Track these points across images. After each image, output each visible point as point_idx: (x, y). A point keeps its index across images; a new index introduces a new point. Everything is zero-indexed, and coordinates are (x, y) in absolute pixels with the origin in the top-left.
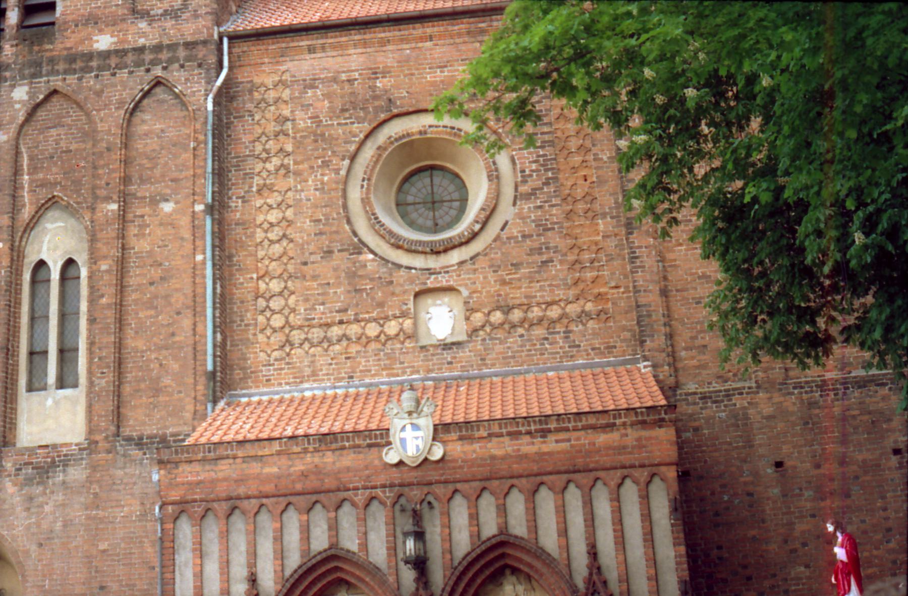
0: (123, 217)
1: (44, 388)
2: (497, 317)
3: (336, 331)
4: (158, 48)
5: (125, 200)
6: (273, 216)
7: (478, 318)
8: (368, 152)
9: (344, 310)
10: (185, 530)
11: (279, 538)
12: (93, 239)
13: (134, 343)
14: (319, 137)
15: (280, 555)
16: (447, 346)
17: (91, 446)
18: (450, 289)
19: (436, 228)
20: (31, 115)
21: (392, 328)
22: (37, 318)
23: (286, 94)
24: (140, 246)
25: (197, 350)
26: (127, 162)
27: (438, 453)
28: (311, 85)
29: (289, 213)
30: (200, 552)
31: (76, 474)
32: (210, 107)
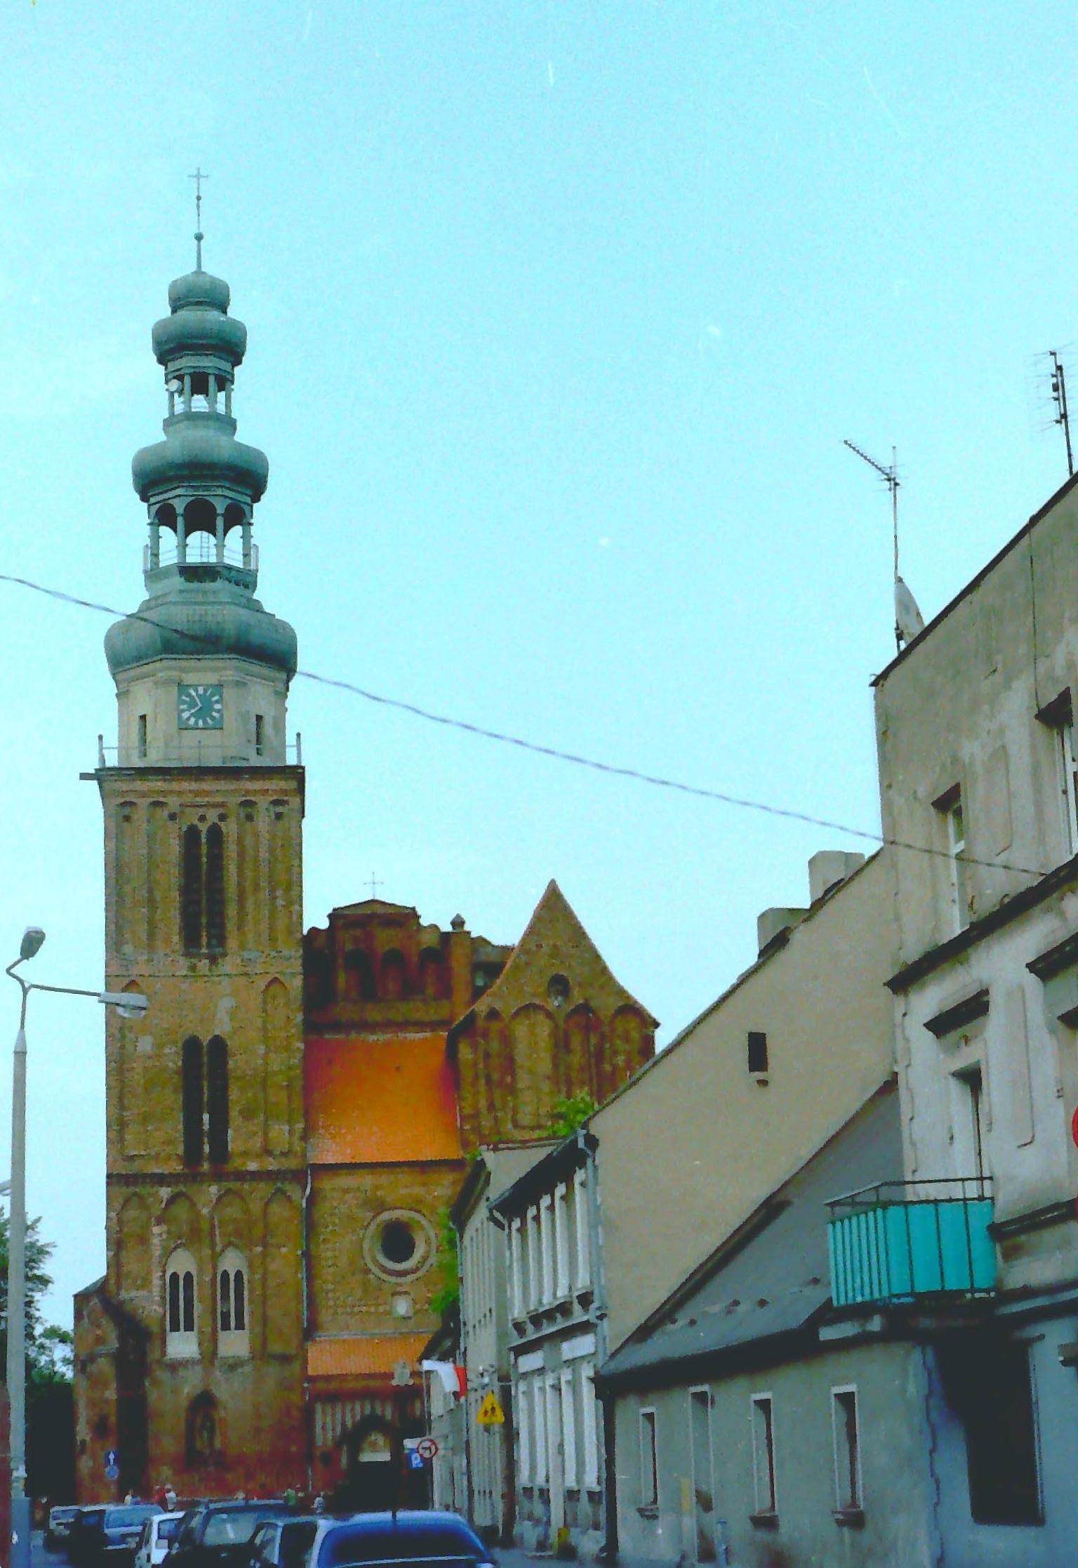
0: (264, 1255)
1: (230, 1329)
2: (426, 1306)
3: (356, 1309)
4: (278, 1172)
5: (265, 1245)
6: (329, 1254)
7: (418, 1307)
8: (373, 1227)
9: (360, 1300)
10: (318, 1407)
11: (353, 1410)
12: (251, 1266)
13: (269, 1313)
14: (351, 1218)
15: (353, 1417)
16: (404, 1318)
17: (253, 1358)
18: (406, 1293)
19: (399, 1261)
20: (219, 1199)
21: (381, 1309)
22: (225, 1297)
23: (335, 1195)
24: (272, 1267)
25: (299, 1317)
26: (266, 1227)
27: (411, 1382)
28: (346, 1191)
29: (337, 1254)
30: (324, 1412)
31: (247, 1369)
32: (304, 1205)
